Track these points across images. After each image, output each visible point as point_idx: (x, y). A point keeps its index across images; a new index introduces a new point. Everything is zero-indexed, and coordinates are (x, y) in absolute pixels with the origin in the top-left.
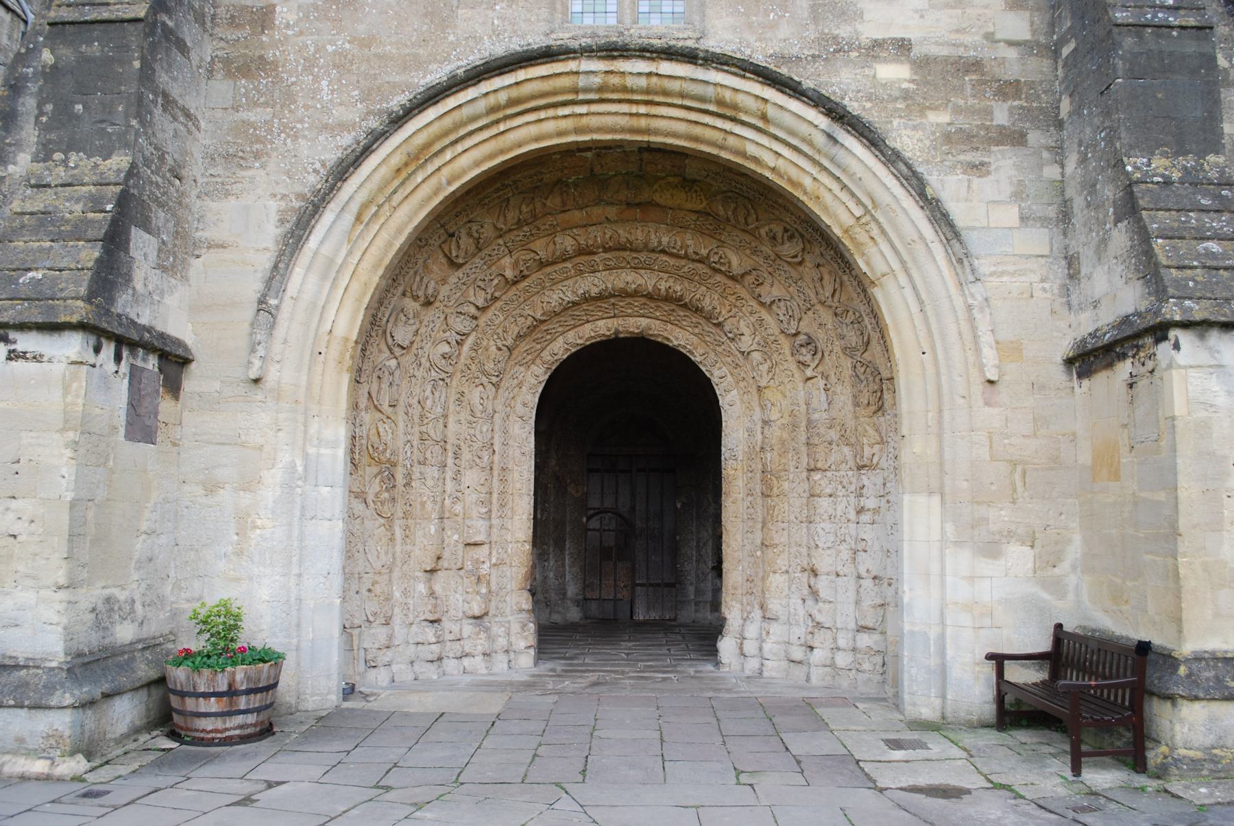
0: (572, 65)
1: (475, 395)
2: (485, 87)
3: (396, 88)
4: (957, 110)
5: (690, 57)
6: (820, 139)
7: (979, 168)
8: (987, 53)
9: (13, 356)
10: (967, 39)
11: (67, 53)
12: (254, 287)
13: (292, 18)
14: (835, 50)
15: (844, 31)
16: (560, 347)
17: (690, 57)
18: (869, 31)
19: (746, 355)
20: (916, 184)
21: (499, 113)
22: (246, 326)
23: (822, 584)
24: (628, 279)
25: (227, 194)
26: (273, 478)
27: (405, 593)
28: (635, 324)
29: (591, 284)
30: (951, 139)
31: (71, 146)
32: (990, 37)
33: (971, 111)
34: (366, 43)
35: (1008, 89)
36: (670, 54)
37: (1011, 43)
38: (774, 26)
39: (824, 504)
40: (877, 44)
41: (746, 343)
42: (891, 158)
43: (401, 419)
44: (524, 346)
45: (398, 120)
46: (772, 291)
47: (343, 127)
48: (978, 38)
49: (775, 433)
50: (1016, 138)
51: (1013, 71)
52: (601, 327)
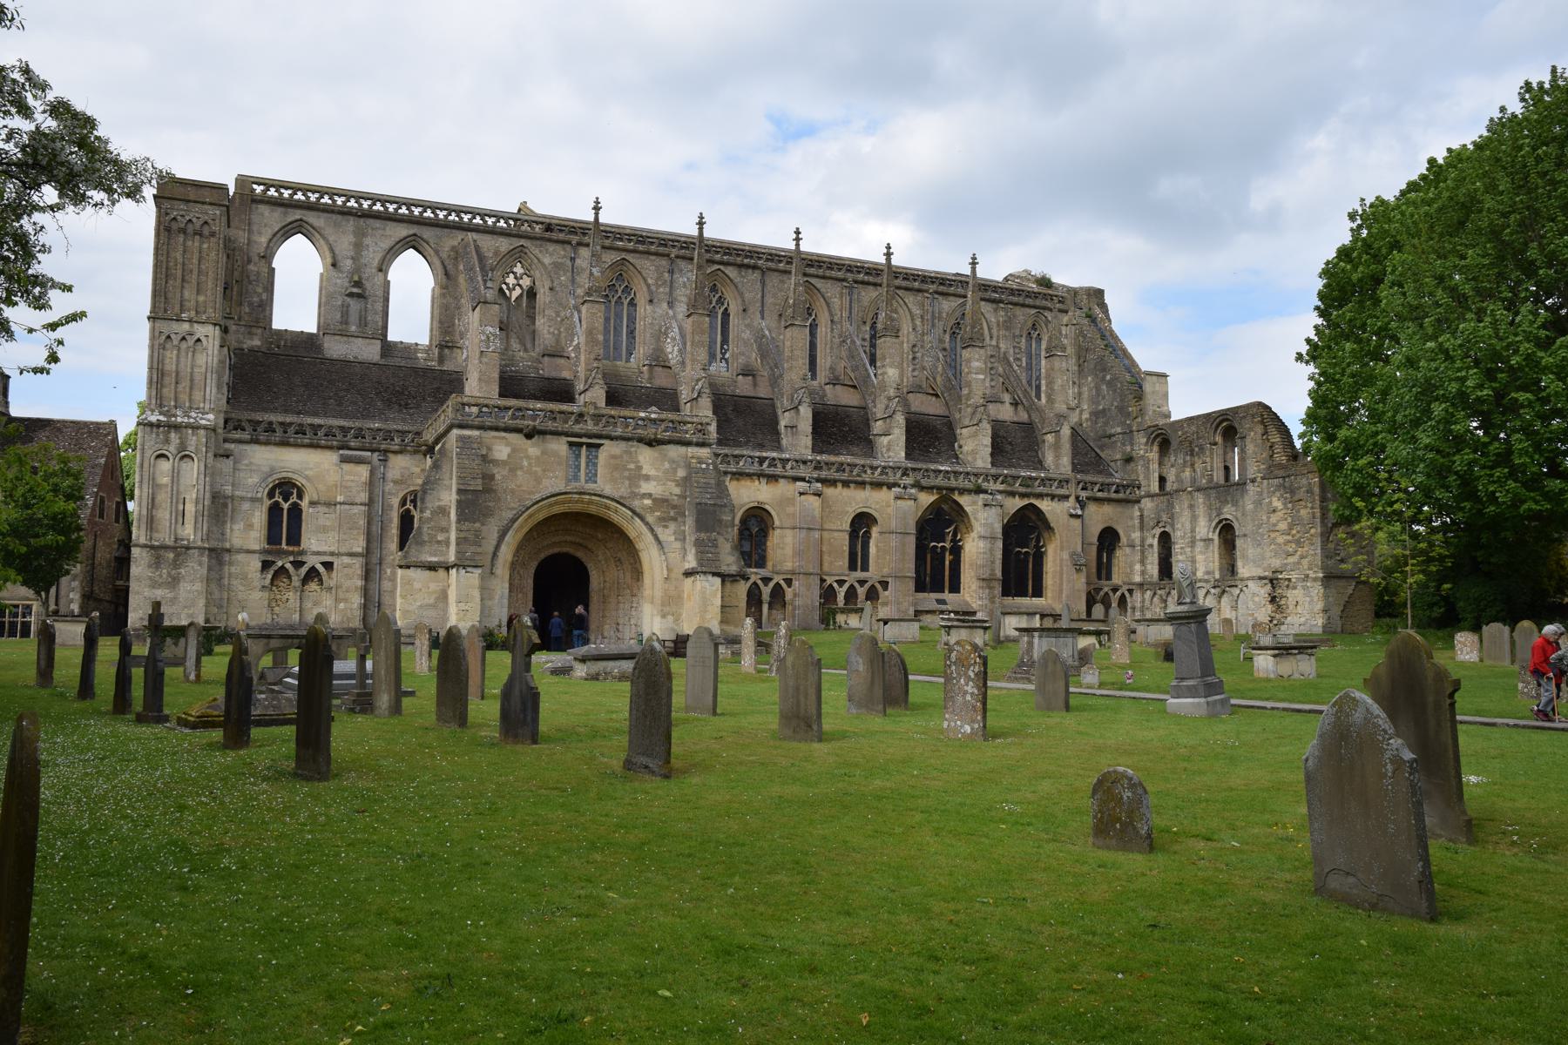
3: (527, 499)
5: (600, 496)
11: (463, 498)
12: (491, 549)
14: (634, 495)
16: (542, 556)
17: (600, 496)
18: (643, 491)
19: (600, 561)
21: (551, 505)
22: (489, 560)
23: (620, 627)
24: (569, 538)
26: (497, 597)
28: (565, 550)
29: (557, 539)
30: (661, 519)
31: (466, 520)
35: (674, 507)
36: (595, 495)
40: (644, 494)
41: (600, 558)
42: (647, 524)
45: (528, 508)
46: (610, 545)
47: (513, 509)
49: (608, 585)
51: (675, 503)
52: (556, 550)
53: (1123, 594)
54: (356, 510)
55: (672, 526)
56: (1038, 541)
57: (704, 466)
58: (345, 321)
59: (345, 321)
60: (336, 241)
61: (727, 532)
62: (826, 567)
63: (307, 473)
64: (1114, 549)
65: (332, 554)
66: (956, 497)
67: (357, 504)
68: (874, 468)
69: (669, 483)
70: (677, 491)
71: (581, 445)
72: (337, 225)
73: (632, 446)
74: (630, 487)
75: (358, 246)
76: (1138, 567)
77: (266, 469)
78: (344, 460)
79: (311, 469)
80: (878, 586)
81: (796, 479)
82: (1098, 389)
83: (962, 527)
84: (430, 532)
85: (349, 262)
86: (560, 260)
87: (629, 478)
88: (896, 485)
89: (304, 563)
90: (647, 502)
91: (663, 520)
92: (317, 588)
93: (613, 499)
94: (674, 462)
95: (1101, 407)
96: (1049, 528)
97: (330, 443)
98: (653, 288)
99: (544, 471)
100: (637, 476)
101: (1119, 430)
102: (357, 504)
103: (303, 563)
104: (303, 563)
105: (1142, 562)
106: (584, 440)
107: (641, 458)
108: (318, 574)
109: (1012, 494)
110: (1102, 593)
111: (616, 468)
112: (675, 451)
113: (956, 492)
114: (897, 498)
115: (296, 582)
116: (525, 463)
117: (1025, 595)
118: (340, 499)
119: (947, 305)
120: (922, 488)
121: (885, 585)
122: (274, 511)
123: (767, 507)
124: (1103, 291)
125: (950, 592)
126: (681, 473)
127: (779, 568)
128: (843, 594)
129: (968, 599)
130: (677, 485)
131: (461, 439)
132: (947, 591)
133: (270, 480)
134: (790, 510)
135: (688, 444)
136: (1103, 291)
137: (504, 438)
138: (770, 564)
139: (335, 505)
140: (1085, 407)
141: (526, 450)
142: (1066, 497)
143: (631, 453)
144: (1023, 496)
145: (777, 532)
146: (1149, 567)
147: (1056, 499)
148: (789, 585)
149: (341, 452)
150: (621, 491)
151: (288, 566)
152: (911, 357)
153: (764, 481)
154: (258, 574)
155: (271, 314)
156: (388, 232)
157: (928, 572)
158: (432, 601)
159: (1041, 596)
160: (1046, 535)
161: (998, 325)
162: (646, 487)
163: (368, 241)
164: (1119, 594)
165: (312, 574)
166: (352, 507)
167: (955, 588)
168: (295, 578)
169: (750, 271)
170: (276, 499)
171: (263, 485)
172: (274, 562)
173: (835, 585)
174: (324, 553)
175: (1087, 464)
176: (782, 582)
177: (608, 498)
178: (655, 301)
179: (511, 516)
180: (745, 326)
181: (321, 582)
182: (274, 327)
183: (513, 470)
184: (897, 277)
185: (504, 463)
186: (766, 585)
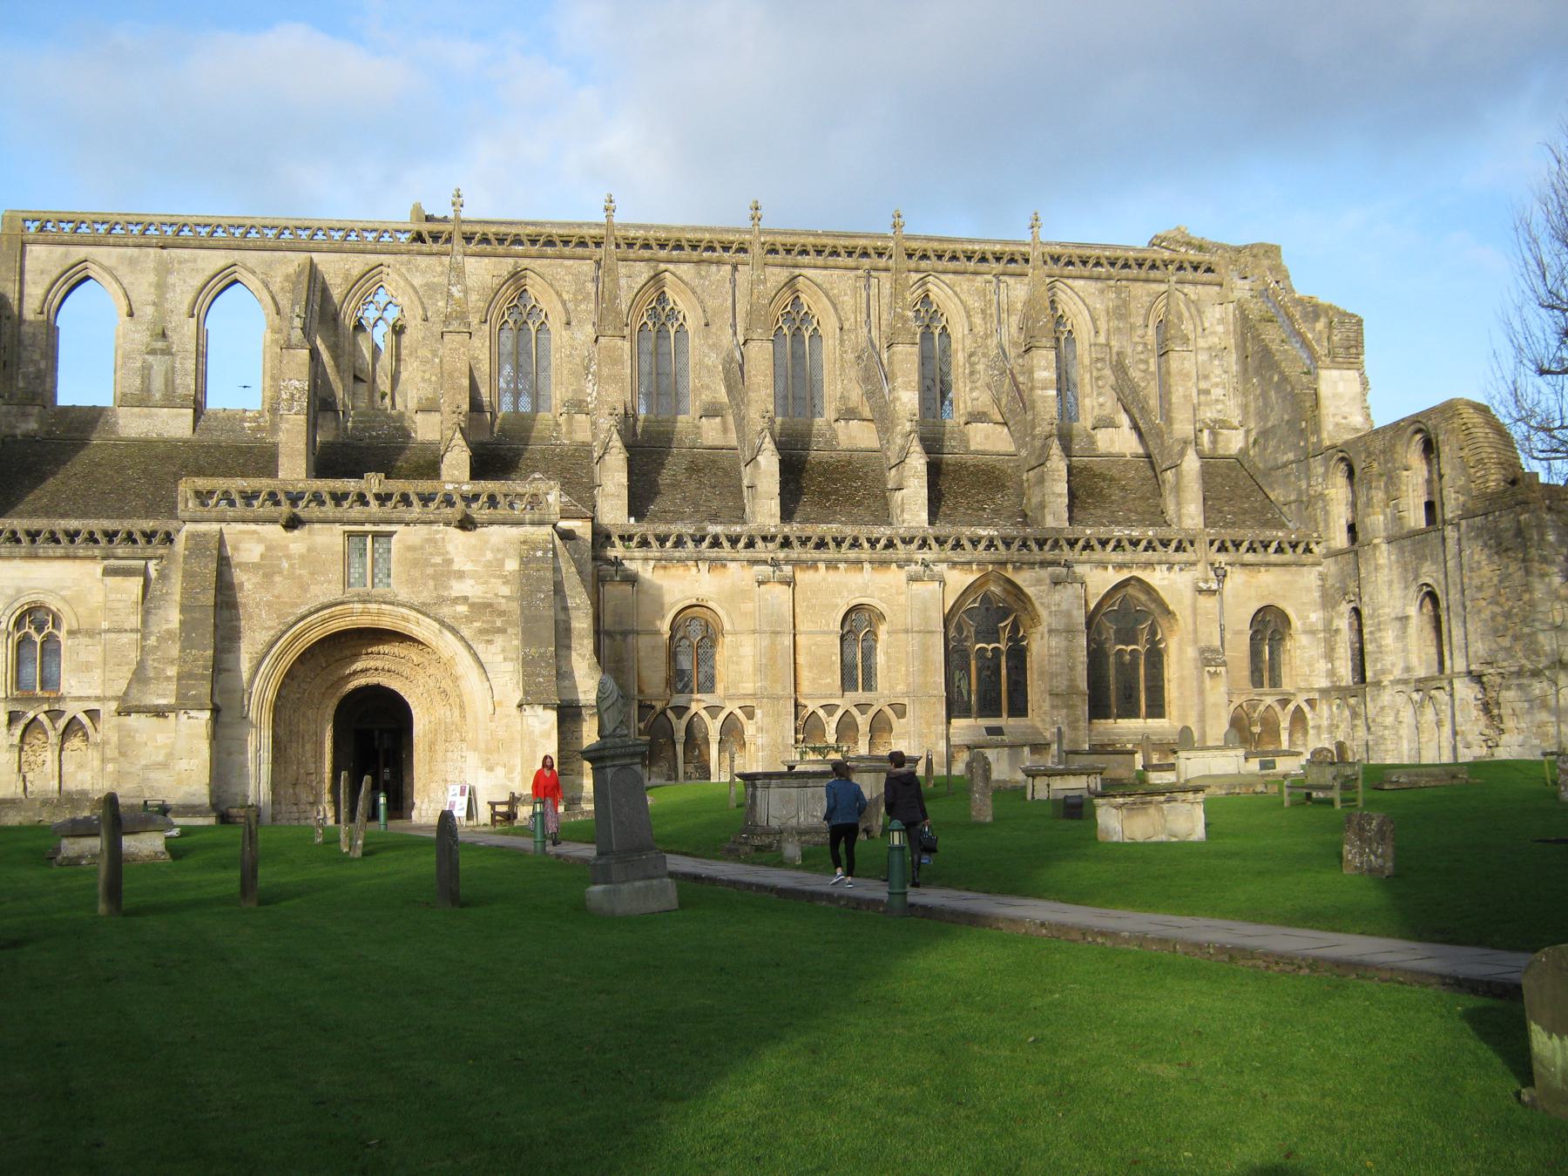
0: (351, 606)
1: (309, 713)
2: (321, 613)
3: (289, 614)
4: (483, 622)
6: (437, 632)
7: (489, 642)
8: (495, 601)
9: (189, 718)
10: (488, 596)
13: (250, 587)
14: (442, 601)
15: (446, 594)
18: (454, 594)
20: (470, 648)
25: (230, 652)
27: (286, 793)
30: (481, 631)
32: (496, 595)
33: (488, 622)
34: (278, 597)
35: (502, 614)
37: (503, 597)
38: (422, 592)
39: (449, 754)
40: (457, 598)
43: (282, 725)
44: (329, 691)
47: (271, 628)
48: (492, 595)
50: (502, 631)
53: (1298, 708)
54: (126, 638)
55: (499, 640)
56: (1153, 633)
57: (539, 554)
58: (146, 389)
59: (146, 389)
60: (132, 284)
61: (582, 645)
62: (805, 686)
63: (62, 593)
64: (1282, 639)
65: (98, 699)
66: (1009, 573)
67: (126, 631)
68: (873, 543)
69: (493, 580)
70: (506, 590)
71: (365, 534)
72: (132, 262)
73: (438, 532)
74: (436, 589)
75: (161, 287)
76: (1322, 666)
77: (11, 592)
78: (108, 572)
79: (69, 588)
80: (890, 712)
81: (754, 562)
82: (1264, 395)
83: (1025, 619)
84: (155, 665)
85: (150, 310)
86: (436, 280)
87: (434, 577)
88: (909, 561)
89: (64, 712)
90: (462, 609)
91: (488, 633)
92: (82, 745)
93: (412, 608)
94: (498, 550)
95: (1270, 424)
96: (1168, 612)
97: (90, 553)
98: (570, 306)
99: (312, 574)
100: (446, 572)
101: (1291, 456)
102: (126, 631)
103: (61, 713)
104: (61, 713)
105: (1330, 655)
106: (368, 527)
107: (450, 548)
108: (82, 727)
109: (1103, 565)
110: (1262, 708)
111: (415, 563)
112: (497, 534)
113: (1010, 567)
114: (913, 579)
115: (53, 737)
116: (285, 565)
117: (1137, 716)
118: (105, 625)
119: (1018, 291)
120: (954, 564)
121: (901, 711)
122: (23, 643)
123: (711, 604)
124: (1278, 248)
125: (1010, 716)
126: (512, 565)
127: (732, 691)
128: (834, 726)
129: (1039, 725)
130: (504, 583)
131: (193, 536)
132: (1005, 715)
133: (17, 605)
134: (748, 607)
135: (520, 523)
136: (1278, 248)
137: (255, 532)
138: (720, 687)
139: (100, 634)
140: (1252, 426)
141: (287, 547)
142: (1194, 564)
143: (435, 541)
144: (1120, 566)
145: (728, 639)
146: (1337, 663)
147: (1176, 568)
148: (750, 716)
149: (106, 562)
150: (425, 595)
151: (42, 717)
152: (967, 371)
153: (704, 566)
154: (4, 730)
155: (55, 387)
156: (200, 265)
157: (974, 687)
158: (161, 758)
159: (1164, 717)
160: (1163, 621)
161: (1108, 313)
162: (458, 588)
163: (172, 279)
164: (1291, 707)
165: (73, 727)
166: (120, 635)
167: (1019, 708)
168: (51, 733)
169: (714, 268)
170: (27, 630)
171: (8, 613)
172: (24, 713)
173: (821, 713)
174: (88, 698)
175: (1245, 512)
176: (738, 712)
177: (403, 606)
178: (573, 324)
179: (267, 639)
180: (709, 346)
181: (86, 735)
182: (62, 400)
183: (268, 576)
184: (910, 256)
185: (255, 567)
186: (714, 717)
